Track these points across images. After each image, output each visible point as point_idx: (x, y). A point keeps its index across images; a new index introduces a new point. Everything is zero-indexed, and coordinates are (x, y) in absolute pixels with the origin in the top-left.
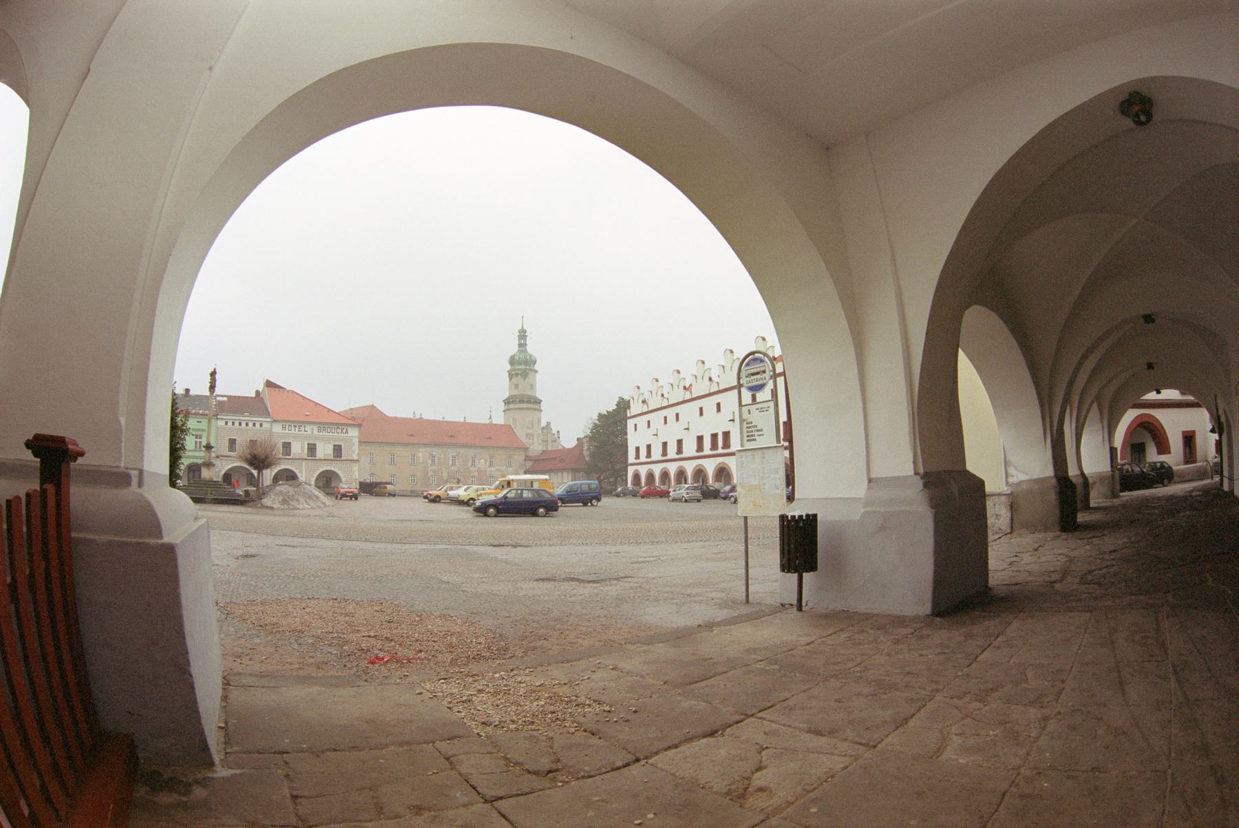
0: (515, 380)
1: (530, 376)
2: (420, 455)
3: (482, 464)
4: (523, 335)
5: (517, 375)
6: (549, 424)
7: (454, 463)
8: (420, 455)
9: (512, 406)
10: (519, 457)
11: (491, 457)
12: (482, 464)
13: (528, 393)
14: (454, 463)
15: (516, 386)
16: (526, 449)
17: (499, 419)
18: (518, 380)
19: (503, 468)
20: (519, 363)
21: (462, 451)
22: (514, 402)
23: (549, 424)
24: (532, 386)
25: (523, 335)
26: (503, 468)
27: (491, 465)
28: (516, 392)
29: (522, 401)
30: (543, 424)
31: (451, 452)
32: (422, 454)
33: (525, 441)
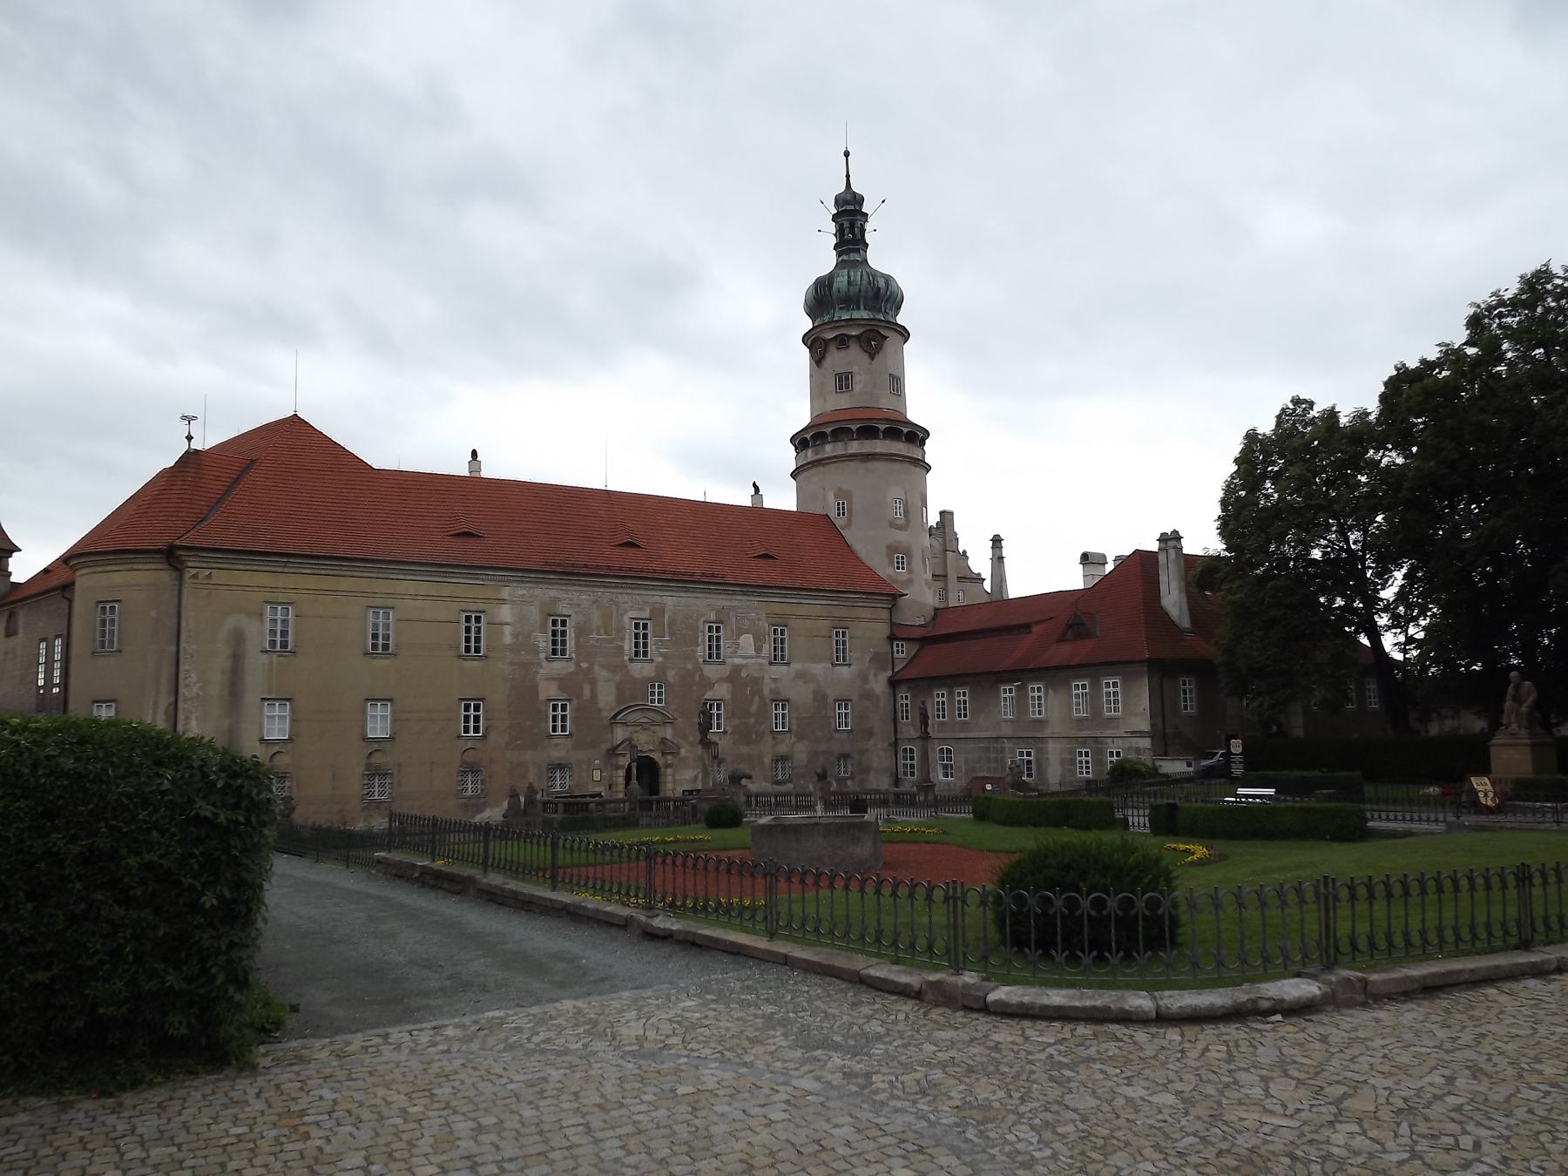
0: (837, 360)
1: (889, 346)
2: (505, 613)
3: (745, 650)
4: (850, 218)
5: (843, 342)
6: (946, 516)
7: (640, 651)
8: (505, 613)
9: (829, 449)
10: (870, 628)
11: (780, 625)
12: (745, 650)
13: (886, 402)
14: (640, 651)
15: (844, 381)
16: (893, 598)
17: (782, 497)
18: (851, 359)
19: (818, 669)
20: (849, 301)
21: (672, 601)
22: (841, 433)
23: (946, 516)
24: (896, 383)
25: (850, 218)
26: (818, 669)
27: (777, 658)
28: (843, 401)
29: (868, 432)
30: (933, 519)
31: (632, 604)
32: (513, 609)
33: (885, 570)
